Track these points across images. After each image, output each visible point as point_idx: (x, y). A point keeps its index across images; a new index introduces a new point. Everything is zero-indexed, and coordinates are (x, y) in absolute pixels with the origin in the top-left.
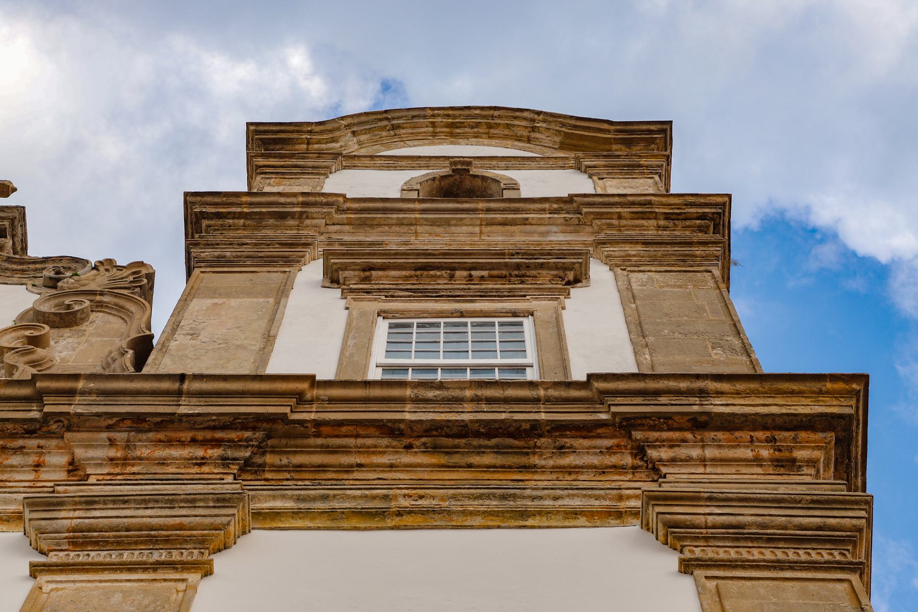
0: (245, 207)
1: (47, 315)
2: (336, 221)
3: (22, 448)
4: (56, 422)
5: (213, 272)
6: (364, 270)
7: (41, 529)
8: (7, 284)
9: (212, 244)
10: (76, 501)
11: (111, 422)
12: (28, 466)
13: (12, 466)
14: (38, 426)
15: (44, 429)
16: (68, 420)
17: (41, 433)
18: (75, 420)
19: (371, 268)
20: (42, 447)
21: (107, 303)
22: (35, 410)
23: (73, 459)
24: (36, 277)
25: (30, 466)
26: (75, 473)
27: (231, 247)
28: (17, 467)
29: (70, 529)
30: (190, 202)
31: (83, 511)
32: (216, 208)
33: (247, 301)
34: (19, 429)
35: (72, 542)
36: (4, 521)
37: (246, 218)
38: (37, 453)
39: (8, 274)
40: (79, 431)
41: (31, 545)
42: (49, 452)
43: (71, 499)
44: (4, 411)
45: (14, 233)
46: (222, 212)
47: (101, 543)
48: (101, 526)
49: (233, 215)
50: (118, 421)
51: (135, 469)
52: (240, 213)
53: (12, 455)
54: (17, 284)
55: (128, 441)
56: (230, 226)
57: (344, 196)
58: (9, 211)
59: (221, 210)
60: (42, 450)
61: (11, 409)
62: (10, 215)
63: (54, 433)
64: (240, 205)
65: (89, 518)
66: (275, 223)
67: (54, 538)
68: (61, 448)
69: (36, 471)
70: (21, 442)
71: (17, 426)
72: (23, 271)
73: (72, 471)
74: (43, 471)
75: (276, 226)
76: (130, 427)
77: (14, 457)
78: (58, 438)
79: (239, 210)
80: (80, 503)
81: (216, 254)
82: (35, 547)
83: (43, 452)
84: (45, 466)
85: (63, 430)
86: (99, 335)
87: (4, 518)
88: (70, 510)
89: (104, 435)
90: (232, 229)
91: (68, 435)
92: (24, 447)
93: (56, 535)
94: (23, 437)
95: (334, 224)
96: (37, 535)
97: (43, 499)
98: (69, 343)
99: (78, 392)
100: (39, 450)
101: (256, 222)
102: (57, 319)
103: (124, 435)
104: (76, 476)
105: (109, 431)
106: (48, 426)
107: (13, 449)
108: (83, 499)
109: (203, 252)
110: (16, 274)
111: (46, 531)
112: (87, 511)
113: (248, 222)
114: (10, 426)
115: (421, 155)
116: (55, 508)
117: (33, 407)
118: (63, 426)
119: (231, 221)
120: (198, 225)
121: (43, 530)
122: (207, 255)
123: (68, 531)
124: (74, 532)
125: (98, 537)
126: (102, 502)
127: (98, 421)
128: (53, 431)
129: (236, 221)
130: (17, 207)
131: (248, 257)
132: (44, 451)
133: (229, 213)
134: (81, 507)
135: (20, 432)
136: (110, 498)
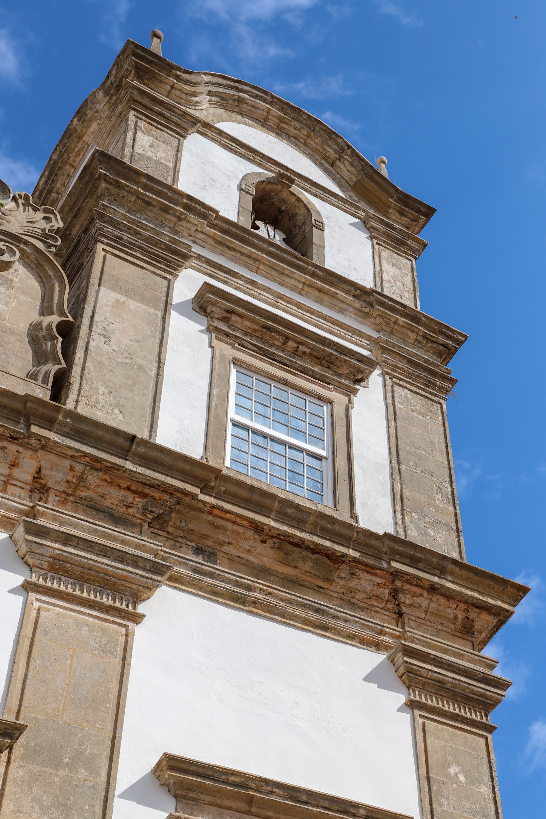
2: (204, 231)
4: (36, 439)
6: (227, 311)
11: (75, 454)
16: (46, 442)
18: (51, 444)
19: (232, 312)
23: (40, 470)
26: (38, 480)
33: (142, 307)
41: (17, 552)
46: (122, 183)
49: (129, 189)
50: (81, 456)
55: (83, 472)
57: (216, 212)
63: (31, 445)
68: (33, 458)
73: (37, 478)
78: (32, 450)
85: (39, 446)
95: (202, 232)
96: (27, 552)
104: (38, 483)
105: (71, 460)
115: (259, 149)
120: (98, 181)
122: (109, 231)
127: (67, 450)
128: (31, 443)
131: (140, 247)
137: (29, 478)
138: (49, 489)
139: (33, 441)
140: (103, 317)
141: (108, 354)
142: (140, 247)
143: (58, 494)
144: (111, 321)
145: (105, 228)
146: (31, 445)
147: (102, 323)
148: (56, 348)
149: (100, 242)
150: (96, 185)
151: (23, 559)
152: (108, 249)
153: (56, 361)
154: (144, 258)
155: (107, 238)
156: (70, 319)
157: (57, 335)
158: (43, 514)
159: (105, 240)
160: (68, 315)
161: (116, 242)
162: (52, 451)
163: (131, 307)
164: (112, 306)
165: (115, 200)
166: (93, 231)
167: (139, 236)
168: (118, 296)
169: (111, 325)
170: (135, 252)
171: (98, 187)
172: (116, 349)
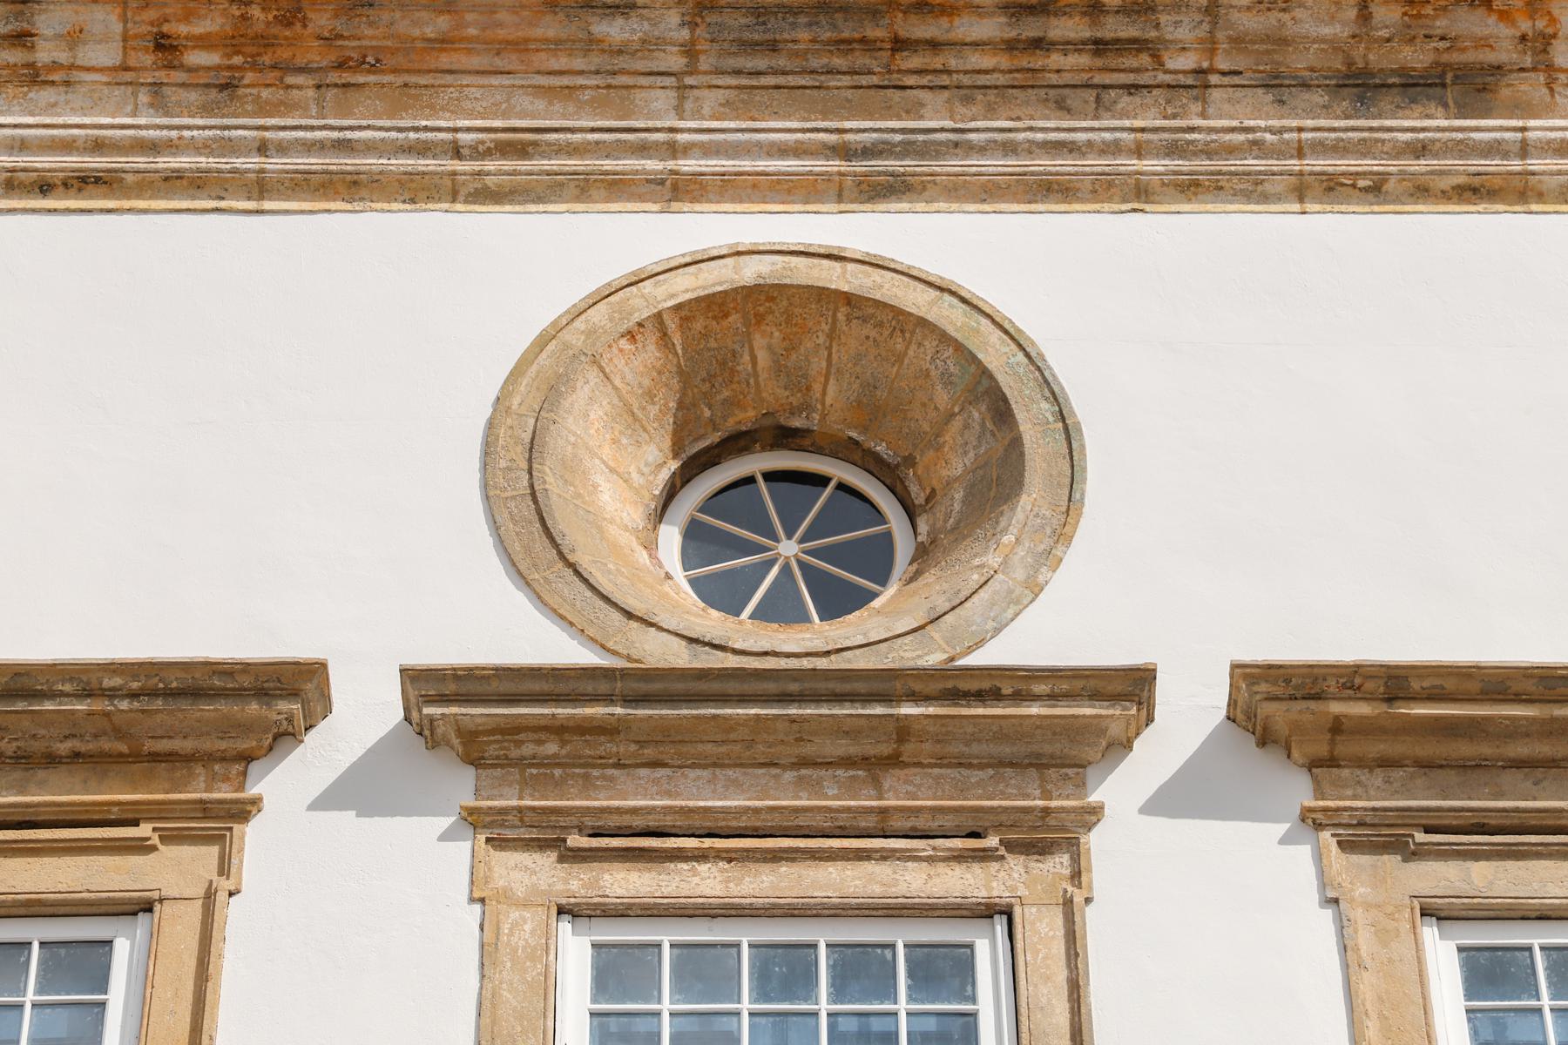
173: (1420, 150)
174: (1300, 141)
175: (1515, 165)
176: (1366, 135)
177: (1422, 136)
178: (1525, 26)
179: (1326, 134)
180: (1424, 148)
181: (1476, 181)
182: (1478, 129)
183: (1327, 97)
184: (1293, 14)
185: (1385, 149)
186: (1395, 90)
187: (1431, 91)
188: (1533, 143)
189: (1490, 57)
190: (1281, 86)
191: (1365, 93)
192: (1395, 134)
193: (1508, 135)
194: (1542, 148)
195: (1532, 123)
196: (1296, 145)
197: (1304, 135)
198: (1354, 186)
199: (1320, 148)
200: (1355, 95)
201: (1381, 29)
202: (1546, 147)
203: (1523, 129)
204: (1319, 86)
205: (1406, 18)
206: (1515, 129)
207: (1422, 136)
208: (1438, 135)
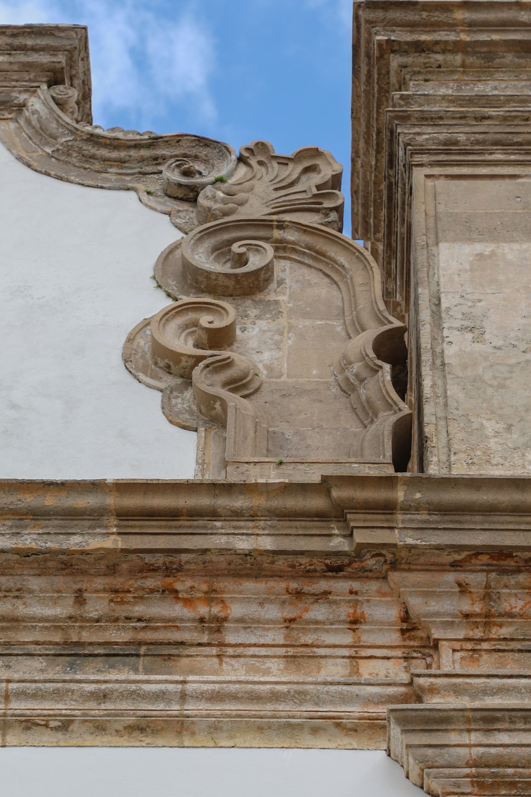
0: (462, 31)
1: (214, 277)
3: (326, 593)
5: (447, 176)
7: (428, 761)
8: (102, 188)
9: (432, 118)
10: (468, 717)
11: (457, 557)
12: (340, 622)
13: (317, 622)
14: (346, 561)
15: (355, 565)
16: (394, 554)
17: (349, 570)
18: (404, 554)
20: (356, 593)
21: (293, 243)
22: (338, 535)
23: (407, 612)
24: (145, 174)
25: (344, 622)
26: (413, 633)
27: (463, 122)
28: (324, 623)
29: (471, 762)
30: (367, 22)
31: (481, 732)
32: (411, 32)
34: (319, 565)
35: (477, 782)
36: (350, 730)
37: (465, 52)
38: (349, 601)
39: (97, 166)
40: (410, 570)
41: (408, 777)
42: (368, 601)
43: (461, 714)
44: (290, 535)
45: (74, 72)
46: (424, 42)
47: (520, 785)
48: (515, 759)
49: (443, 47)
50: (470, 557)
51: (505, 632)
52: (455, 43)
53: (313, 603)
54: (120, 189)
55: (488, 586)
56: (439, 66)
58: (62, 34)
59: (424, 37)
60: (357, 597)
61: (300, 532)
62: (66, 42)
63: (371, 571)
64: (451, 26)
65: (495, 746)
66: (517, 60)
67: (450, 776)
68: (385, 595)
69: (354, 630)
70: (323, 585)
71: (315, 561)
72: (121, 162)
73: (408, 630)
74: (364, 631)
75: (519, 66)
76: (488, 565)
77: (316, 606)
78: (377, 578)
79: (452, 37)
80: (475, 720)
81: (442, 137)
82: (419, 784)
83: (358, 601)
84: (365, 622)
85: (385, 567)
86: (305, 315)
87: (349, 726)
88: (461, 731)
89: (451, 577)
90: (444, 72)
91: (394, 576)
92: (330, 593)
93: (452, 771)
94: (325, 576)
96: (423, 770)
97: (419, 713)
98: (264, 332)
99: (398, 507)
100: (352, 597)
101: (484, 58)
102: (231, 283)
103: (481, 578)
104: (414, 638)
105: (455, 571)
106: (362, 562)
107: (314, 595)
108: (479, 714)
109: (418, 134)
110: (111, 166)
111: (436, 764)
112: (488, 734)
113: (470, 60)
114: (304, 560)
116: (440, 728)
117: (333, 528)
118: (386, 561)
119: (440, 57)
120: (383, 62)
121: (430, 763)
122: (427, 140)
123: (468, 765)
124: (476, 766)
125: (514, 775)
126: (507, 720)
127: (439, 556)
128: (369, 567)
129: (449, 57)
130: (75, 28)
131: (496, 143)
132: (360, 599)
133: (437, 43)
134: (477, 727)
135: (318, 568)
136: (519, 714)
137: (395, 638)
138: (437, 642)
139: (370, 563)
140: (457, 296)
141: (486, 359)
142: (496, 143)
143: (457, 646)
144: (476, 296)
145: (418, 138)
146: (371, 571)
147: (459, 307)
148: (385, 386)
149: (417, 165)
150: (384, 71)
151: (422, 788)
152: (436, 171)
153: (391, 410)
154: (512, 157)
155: (429, 152)
156: (397, 323)
157: (379, 362)
158: (433, 690)
159: (425, 158)
160: (392, 318)
161: (448, 152)
162: (413, 567)
163: (510, 257)
164: (472, 270)
165: (426, 80)
166: (401, 153)
167: (486, 122)
168: (478, 247)
169: (479, 304)
170: (491, 154)
171: (388, 72)
172: (500, 343)
173: (104, 696)
174: (7, 691)
175: (175, 708)
176: (59, 685)
177: (103, 686)
178: (203, 610)
179: (28, 685)
180: (105, 696)
181: (143, 723)
182: (148, 682)
183: (45, 664)
184: (25, 600)
185: (74, 697)
186: (100, 659)
187: (127, 659)
188: (189, 693)
189: (177, 636)
190: (11, 655)
191: (76, 660)
192: (83, 685)
193: (171, 687)
194: (197, 697)
195: (191, 678)
196: (4, 694)
197: (13, 686)
198: (46, 726)
199: (22, 695)
200: (68, 662)
201: (92, 612)
202: (200, 697)
203: (184, 682)
204: (40, 655)
205: (112, 604)
206: (177, 682)
207: (103, 686)
208: (117, 686)
